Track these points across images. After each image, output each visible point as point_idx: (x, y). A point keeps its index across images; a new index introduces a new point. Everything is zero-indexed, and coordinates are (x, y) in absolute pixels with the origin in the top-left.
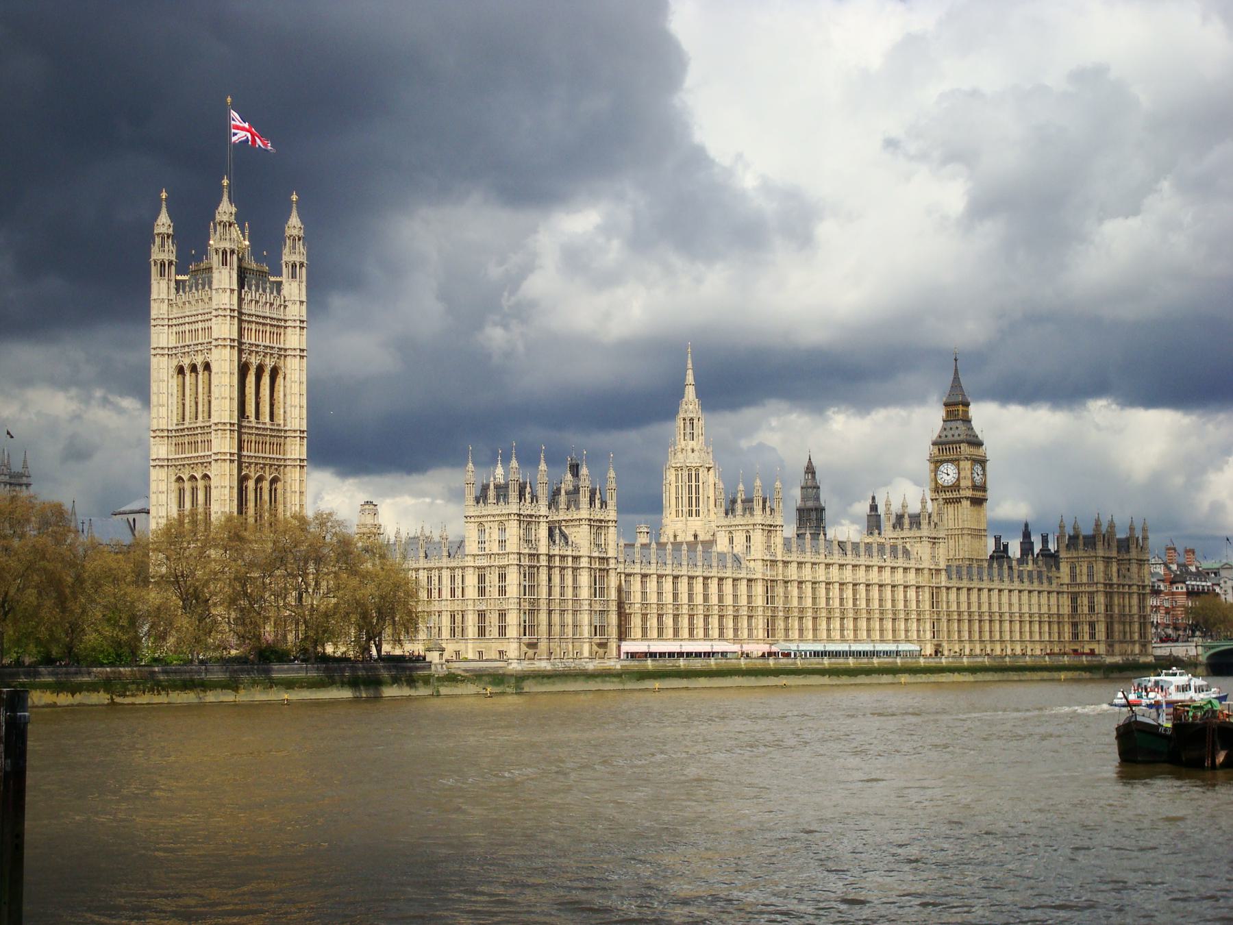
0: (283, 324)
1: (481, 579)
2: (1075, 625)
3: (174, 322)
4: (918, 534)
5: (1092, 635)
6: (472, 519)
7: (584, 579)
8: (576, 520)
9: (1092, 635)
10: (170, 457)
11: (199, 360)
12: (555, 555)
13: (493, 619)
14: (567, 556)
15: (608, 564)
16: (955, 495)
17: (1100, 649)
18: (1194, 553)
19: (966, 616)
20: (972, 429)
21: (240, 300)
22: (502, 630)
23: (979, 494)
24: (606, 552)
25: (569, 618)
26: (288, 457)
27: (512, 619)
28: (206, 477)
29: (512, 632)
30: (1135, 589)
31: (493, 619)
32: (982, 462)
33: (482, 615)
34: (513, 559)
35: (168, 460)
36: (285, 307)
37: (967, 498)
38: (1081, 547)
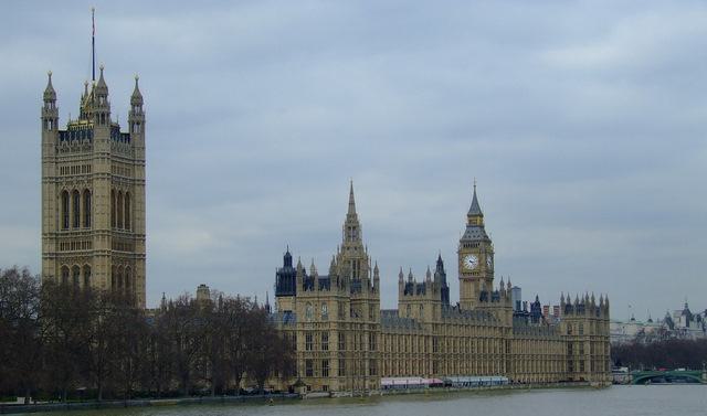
1: (309, 338)
2: (571, 362)
4: (497, 305)
5: (582, 369)
7: (366, 338)
9: (582, 369)
11: (80, 188)
13: (318, 365)
17: (589, 377)
22: (326, 373)
25: (358, 364)
27: (334, 366)
28: (86, 267)
29: (334, 372)
31: (318, 365)
32: (492, 254)
33: (309, 363)
34: (333, 326)
38: (575, 312)
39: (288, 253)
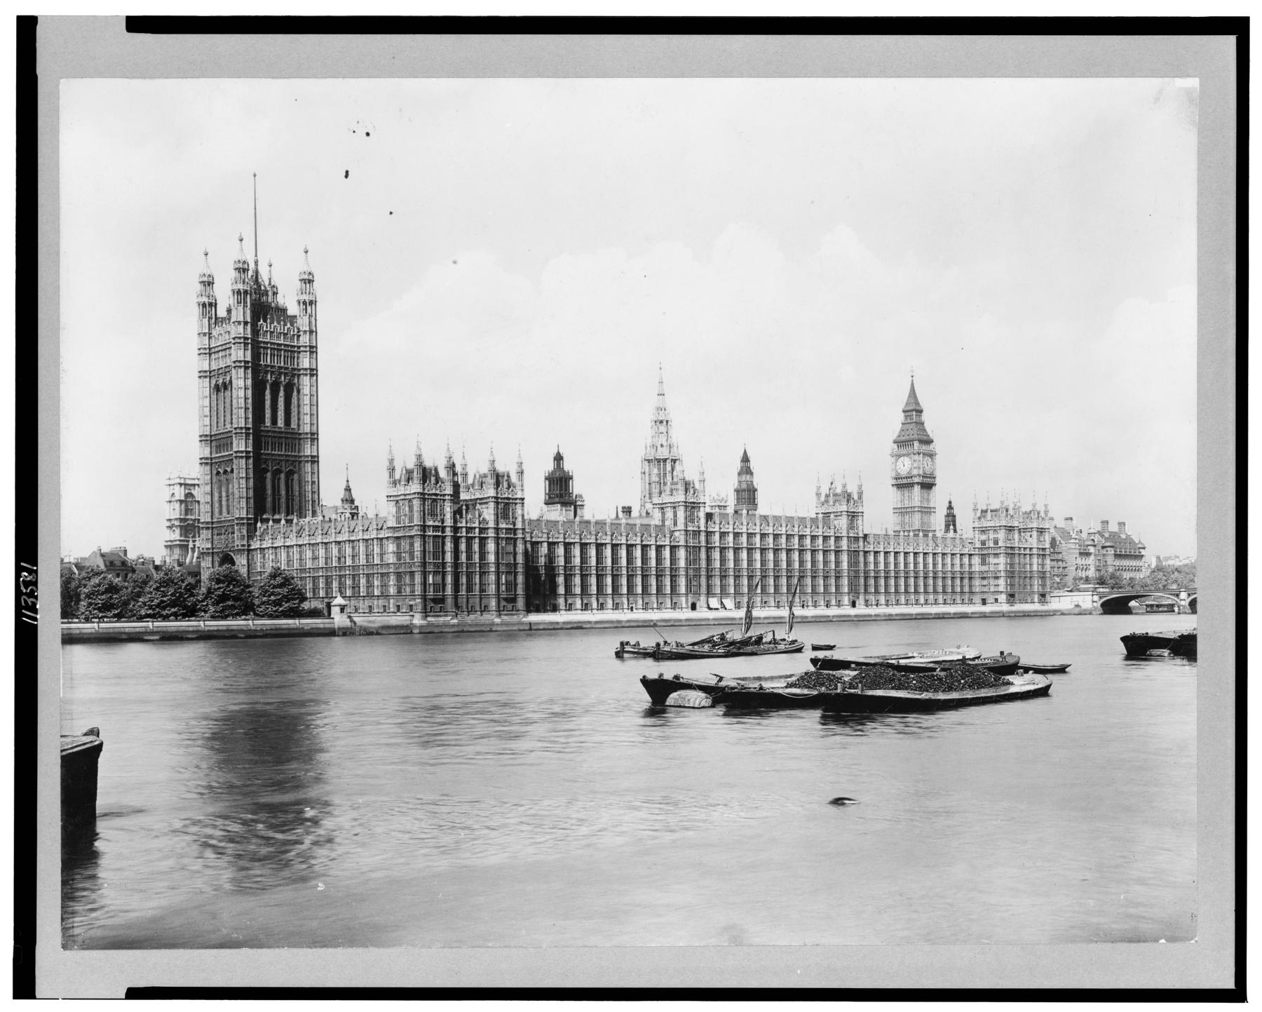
0: (296, 349)
3: (213, 350)
6: (392, 499)
8: (486, 498)
10: (213, 456)
12: (462, 527)
14: (475, 528)
15: (515, 534)
16: (909, 481)
18: (1124, 525)
19: (912, 574)
20: (925, 430)
21: (255, 332)
23: (928, 480)
24: (514, 524)
26: (302, 454)
30: (1035, 551)
35: (211, 459)
36: (299, 336)
37: (918, 483)
39: (558, 454)
